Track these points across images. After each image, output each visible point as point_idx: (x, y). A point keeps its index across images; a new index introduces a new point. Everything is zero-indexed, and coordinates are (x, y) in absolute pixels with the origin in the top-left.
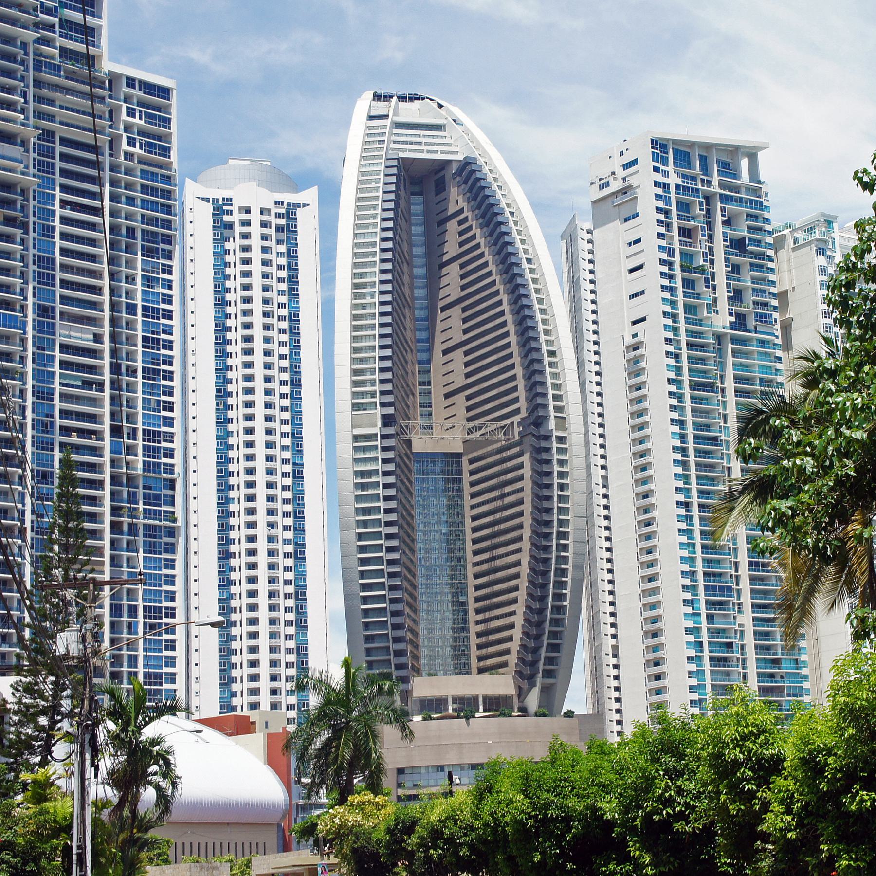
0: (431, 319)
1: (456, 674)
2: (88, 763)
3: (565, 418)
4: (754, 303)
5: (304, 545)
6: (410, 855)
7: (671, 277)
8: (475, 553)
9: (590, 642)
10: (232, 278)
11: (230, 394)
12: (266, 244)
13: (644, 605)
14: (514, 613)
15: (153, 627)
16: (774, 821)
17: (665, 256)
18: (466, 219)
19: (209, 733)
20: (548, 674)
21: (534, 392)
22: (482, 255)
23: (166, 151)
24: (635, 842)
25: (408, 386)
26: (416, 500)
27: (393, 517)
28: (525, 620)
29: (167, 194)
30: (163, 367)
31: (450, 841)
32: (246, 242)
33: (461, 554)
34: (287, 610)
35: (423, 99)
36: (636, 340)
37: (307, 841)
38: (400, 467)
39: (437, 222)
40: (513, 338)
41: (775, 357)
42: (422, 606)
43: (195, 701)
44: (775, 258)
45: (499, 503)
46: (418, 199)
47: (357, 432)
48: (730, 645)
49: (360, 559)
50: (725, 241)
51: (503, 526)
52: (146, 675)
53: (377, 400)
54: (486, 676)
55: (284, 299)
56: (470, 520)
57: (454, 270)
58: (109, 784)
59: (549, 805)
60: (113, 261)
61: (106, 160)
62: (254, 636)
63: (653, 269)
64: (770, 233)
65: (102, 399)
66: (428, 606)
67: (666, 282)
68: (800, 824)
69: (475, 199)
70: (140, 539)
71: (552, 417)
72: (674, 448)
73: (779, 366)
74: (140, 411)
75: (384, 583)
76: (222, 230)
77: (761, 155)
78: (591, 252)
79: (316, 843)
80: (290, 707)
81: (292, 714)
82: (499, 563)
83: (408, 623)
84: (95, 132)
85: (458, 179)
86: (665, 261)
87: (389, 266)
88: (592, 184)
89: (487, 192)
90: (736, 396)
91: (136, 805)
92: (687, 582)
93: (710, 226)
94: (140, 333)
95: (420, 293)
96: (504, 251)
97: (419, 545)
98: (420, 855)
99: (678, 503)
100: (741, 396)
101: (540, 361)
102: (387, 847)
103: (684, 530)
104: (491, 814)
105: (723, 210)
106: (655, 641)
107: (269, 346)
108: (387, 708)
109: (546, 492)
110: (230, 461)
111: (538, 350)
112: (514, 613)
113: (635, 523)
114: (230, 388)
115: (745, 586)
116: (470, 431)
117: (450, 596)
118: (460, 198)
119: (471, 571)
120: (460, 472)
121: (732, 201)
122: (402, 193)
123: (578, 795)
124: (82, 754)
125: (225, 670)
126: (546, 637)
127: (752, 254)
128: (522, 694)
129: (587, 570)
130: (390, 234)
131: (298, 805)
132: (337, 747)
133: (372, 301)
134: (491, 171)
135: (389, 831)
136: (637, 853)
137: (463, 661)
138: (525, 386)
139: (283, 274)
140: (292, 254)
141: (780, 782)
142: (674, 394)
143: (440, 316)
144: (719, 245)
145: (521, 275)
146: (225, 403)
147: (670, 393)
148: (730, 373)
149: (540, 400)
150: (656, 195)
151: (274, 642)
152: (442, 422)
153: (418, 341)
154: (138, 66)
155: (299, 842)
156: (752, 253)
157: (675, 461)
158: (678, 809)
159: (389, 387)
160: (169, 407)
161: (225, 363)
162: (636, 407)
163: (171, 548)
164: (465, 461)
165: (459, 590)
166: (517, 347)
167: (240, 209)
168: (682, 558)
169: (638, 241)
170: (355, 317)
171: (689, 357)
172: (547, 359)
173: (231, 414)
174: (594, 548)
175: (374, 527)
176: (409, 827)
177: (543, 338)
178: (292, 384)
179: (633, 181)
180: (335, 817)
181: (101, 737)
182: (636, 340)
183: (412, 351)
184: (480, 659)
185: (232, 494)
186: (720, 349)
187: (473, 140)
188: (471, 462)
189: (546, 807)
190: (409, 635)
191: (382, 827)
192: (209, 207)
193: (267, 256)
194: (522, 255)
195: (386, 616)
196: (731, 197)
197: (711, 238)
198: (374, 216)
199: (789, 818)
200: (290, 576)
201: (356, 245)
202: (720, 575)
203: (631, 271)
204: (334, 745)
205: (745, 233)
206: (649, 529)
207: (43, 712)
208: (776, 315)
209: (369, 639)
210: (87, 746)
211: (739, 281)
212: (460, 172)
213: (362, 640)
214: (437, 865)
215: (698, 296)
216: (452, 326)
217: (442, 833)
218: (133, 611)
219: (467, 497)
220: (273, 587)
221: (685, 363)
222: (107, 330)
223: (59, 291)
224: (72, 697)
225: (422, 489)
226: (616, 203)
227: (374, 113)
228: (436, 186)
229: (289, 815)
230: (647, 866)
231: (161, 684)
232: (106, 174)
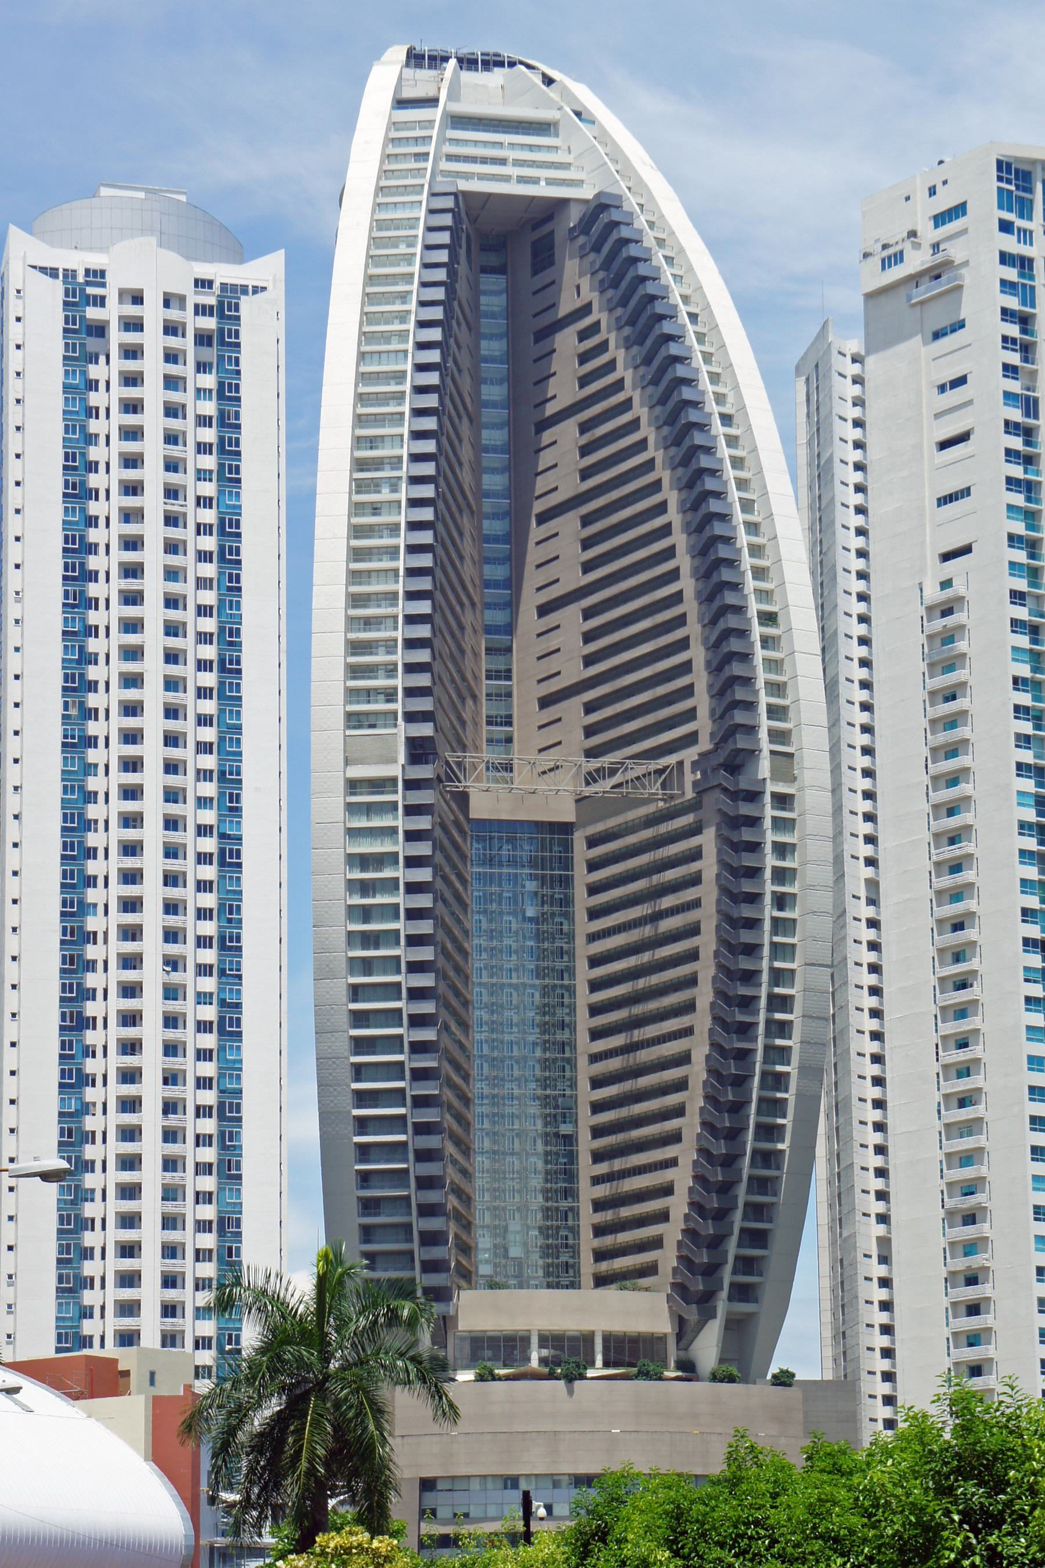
0: (516, 541)
1: (549, 1286)
3: (791, 756)
5: (238, 1005)
8: (596, 1034)
9: (831, 1229)
10: (102, 440)
11: (92, 686)
12: (174, 369)
13: (948, 1155)
14: (672, 1163)
17: (1016, 415)
18: (595, 328)
19: (33, 1391)
20: (742, 1293)
21: (728, 698)
25: (464, 678)
26: (474, 920)
27: (426, 954)
32: (132, 365)
35: (512, 64)
36: (949, 593)
38: (443, 849)
40: (687, 584)
42: (481, 1142)
45: (647, 931)
51: (655, 979)
53: (398, 707)
54: (611, 1294)
55: (208, 489)
57: (566, 436)
66: (494, 1142)
67: (1017, 471)
69: (615, 284)
71: (765, 753)
76: (83, 337)
80: (201, 1343)
81: (206, 1357)
82: (644, 1056)
83: (452, 1175)
85: (582, 240)
86: (1017, 425)
87: (430, 423)
88: (866, 255)
89: (642, 269)
95: (494, 482)
96: (675, 398)
97: (478, 1014)
101: (743, 633)
106: (969, 1232)
107: (176, 588)
108: (402, 1355)
109: (747, 911)
110: (89, 825)
111: (740, 610)
112: (672, 1163)
113: (933, 981)
116: (591, 778)
118: (585, 283)
119: (585, 1071)
120: (567, 863)
122: (462, 268)
125: (69, 1261)
128: (684, 1333)
130: (434, 356)
131: (212, 1548)
133: (394, 496)
134: (651, 224)
137: (564, 1258)
138: (710, 686)
139: (209, 435)
140: (228, 394)
142: (1026, 710)
143: (536, 532)
145: (709, 450)
146: (82, 704)
147: (1017, 708)
149: (740, 717)
150: (1004, 283)
151: (171, 1207)
152: (533, 756)
153: (487, 584)
157: (1023, 853)
159: (423, 680)
161: (83, 620)
162: (943, 737)
164: (579, 839)
165: (558, 1111)
166: (695, 605)
167: (122, 293)
169: (960, 381)
172: (757, 630)
175: (385, 973)
177: (750, 584)
178: (222, 669)
179: (956, 252)
182: (949, 593)
183: (473, 604)
184: (600, 1256)
185: (93, 895)
187: (617, 155)
188: (593, 842)
190: (453, 1202)
192: (58, 287)
193: (175, 397)
194: (713, 408)
200: (208, 1069)
201: (363, 377)
203: (944, 445)
206: (963, 996)
209: (369, 1206)
212: (586, 224)
213: (354, 1206)
216: (559, 554)
219: (580, 915)
220: (173, 1092)
226: (917, 299)
227: (408, 93)
228: (535, 255)
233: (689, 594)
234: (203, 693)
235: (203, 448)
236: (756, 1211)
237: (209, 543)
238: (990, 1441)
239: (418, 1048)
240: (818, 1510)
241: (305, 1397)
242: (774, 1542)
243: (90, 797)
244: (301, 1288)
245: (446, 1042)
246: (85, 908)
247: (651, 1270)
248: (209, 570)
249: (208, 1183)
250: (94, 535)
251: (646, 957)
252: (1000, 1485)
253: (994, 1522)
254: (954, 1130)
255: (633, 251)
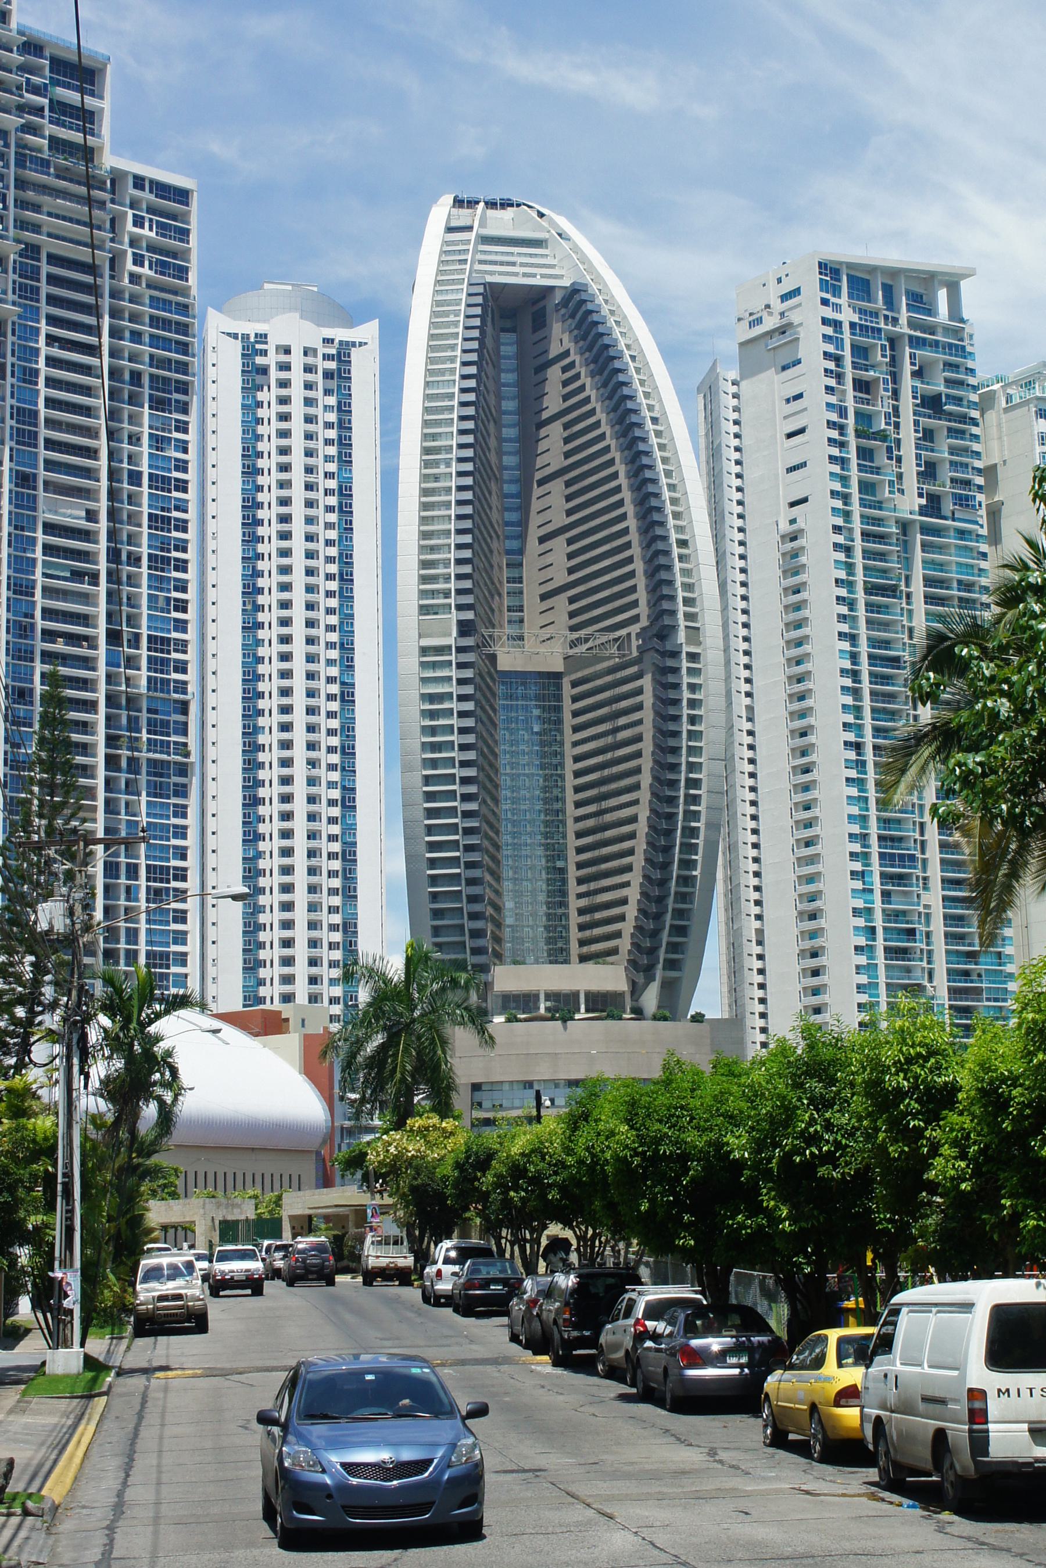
0: (525, 496)
1: (551, 962)
2: (76, 1069)
3: (698, 629)
4: (952, 480)
5: (354, 790)
6: (484, 1197)
7: (842, 445)
8: (578, 805)
9: (727, 924)
10: (266, 438)
11: (260, 591)
12: (311, 394)
13: (799, 877)
14: (627, 884)
15: (158, 892)
16: (944, 1167)
17: (834, 417)
18: (572, 365)
19: (229, 1031)
20: (672, 965)
21: (658, 594)
22: (592, 412)
23: (182, 273)
24: (770, 1190)
25: (493, 583)
26: (501, 734)
27: (471, 755)
28: (642, 894)
29: (184, 329)
30: (175, 554)
31: (536, 1180)
32: (284, 392)
33: (559, 805)
34: (332, 874)
35: (518, 205)
36: (795, 527)
37: (353, 1174)
38: (481, 690)
39: (535, 367)
40: (632, 523)
41: (979, 553)
42: (507, 873)
43: (211, 990)
44: (980, 421)
45: (610, 739)
46: (511, 337)
47: (426, 642)
48: (911, 932)
49: (427, 809)
50: (914, 397)
52: (149, 955)
53: (452, 601)
54: (590, 967)
55: (332, 467)
56: (573, 762)
57: (555, 432)
58: (102, 1096)
59: (661, 1139)
60: (113, 415)
61: (106, 283)
62: (288, 906)
63: (820, 434)
64: (975, 388)
65: (96, 596)
66: (515, 873)
67: (835, 452)
68: (977, 1173)
69: (584, 338)
70: (143, 778)
71: (682, 628)
72: (842, 671)
73: (983, 565)
74: (145, 611)
75: (457, 841)
76: (254, 376)
77: (963, 284)
78: (736, 409)
79: (365, 1178)
80: (333, 1001)
81: (337, 1009)
82: (608, 818)
83: (489, 893)
84: (93, 246)
85: (563, 311)
86: (834, 423)
87: (470, 425)
88: (739, 320)
90: (926, 603)
91: (135, 1123)
92: (857, 848)
93: (895, 377)
94: (145, 510)
95: (510, 460)
96: (622, 408)
97: (504, 793)
98: (496, 1196)
99: (846, 743)
100: (932, 604)
101: (667, 553)
102: (455, 1186)
103: (853, 780)
104: (587, 1149)
105: (912, 356)
107: (312, 529)
108: (459, 1006)
109: (672, 727)
110: (259, 678)
111: (665, 538)
112: (627, 884)
113: (789, 769)
114: (261, 582)
115: (933, 854)
116: (573, 644)
117: (543, 861)
118: (566, 338)
119: (571, 827)
120: (559, 698)
121: (924, 345)
122: (489, 329)
123: (697, 1128)
124: (69, 1058)
125: (250, 950)
126: (669, 916)
127: (950, 416)
128: (636, 990)
129: (724, 831)
130: (472, 383)
131: (342, 1128)
132: (395, 1055)
133: (448, 470)
134: (606, 302)
135: (458, 1166)
136: (772, 1203)
137: (560, 945)
138: (647, 586)
139: (332, 434)
140: (344, 409)
141: (954, 1118)
142: (844, 599)
143: (537, 491)
144: (908, 404)
145: (644, 440)
146: (254, 602)
147: (838, 598)
148: (918, 572)
149: (666, 605)
150: (824, 336)
151: (313, 916)
152: (537, 631)
153: (507, 524)
154: (148, 162)
155: (343, 1176)
156: (950, 414)
157: (843, 688)
158: (825, 1148)
159: (467, 584)
160: (182, 606)
161: (255, 550)
162: (793, 616)
163: (182, 791)
164: (566, 683)
165: (555, 853)
166: (637, 535)
167: (278, 348)
168: (850, 816)
169: (799, 396)
170: (425, 492)
171: (864, 551)
172: (676, 551)
173: (261, 617)
174: (734, 800)
175: (445, 768)
176: (483, 1161)
177: (671, 522)
178: (342, 579)
179: (795, 317)
180: (390, 1145)
181: (94, 1035)
182: (795, 527)
183: (498, 537)
184: (582, 943)
185: (261, 721)
186: (905, 542)
187: (584, 259)
188: (575, 684)
189: (658, 1141)
190: (490, 911)
191: (450, 1161)
192: (238, 344)
194: (647, 414)
195: (460, 885)
196: (924, 339)
197: (896, 394)
198: (452, 360)
199: (963, 1164)
200: (336, 829)
201: (428, 397)
202: (901, 839)
203: (790, 436)
204: (390, 1052)
205: (942, 388)
206: (807, 778)
207: (20, 1001)
208: (980, 497)
209: (437, 914)
210: (75, 1048)
211: (932, 451)
213: (428, 915)
214: (520, 1210)
215: (877, 471)
216: (551, 505)
217: (526, 1170)
218: (133, 871)
219: (567, 730)
221: (858, 559)
222: (103, 505)
223: (43, 453)
224: (56, 984)
225: (509, 720)
226: (771, 347)
227: (453, 224)
228: (534, 321)
229: (332, 1140)
230: (785, 1220)
231: (168, 967)
232: (106, 302)
233: (633, 528)
234: (329, 594)
235: (328, 442)
236: (679, 914)
237: (333, 501)
238: (827, 1053)
239: (467, 814)
240: (720, 1099)
241: (398, 1034)
242: (692, 1118)
243: (260, 660)
244: (395, 967)
245: (484, 810)
246: (257, 730)
247: (614, 951)
248: (333, 518)
249: (336, 901)
250: (261, 497)
251: (609, 756)
252: (832, 1081)
253: (829, 1104)
254: (802, 861)
255: (595, 317)
